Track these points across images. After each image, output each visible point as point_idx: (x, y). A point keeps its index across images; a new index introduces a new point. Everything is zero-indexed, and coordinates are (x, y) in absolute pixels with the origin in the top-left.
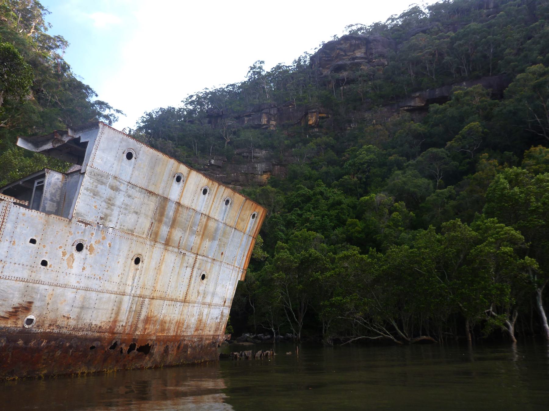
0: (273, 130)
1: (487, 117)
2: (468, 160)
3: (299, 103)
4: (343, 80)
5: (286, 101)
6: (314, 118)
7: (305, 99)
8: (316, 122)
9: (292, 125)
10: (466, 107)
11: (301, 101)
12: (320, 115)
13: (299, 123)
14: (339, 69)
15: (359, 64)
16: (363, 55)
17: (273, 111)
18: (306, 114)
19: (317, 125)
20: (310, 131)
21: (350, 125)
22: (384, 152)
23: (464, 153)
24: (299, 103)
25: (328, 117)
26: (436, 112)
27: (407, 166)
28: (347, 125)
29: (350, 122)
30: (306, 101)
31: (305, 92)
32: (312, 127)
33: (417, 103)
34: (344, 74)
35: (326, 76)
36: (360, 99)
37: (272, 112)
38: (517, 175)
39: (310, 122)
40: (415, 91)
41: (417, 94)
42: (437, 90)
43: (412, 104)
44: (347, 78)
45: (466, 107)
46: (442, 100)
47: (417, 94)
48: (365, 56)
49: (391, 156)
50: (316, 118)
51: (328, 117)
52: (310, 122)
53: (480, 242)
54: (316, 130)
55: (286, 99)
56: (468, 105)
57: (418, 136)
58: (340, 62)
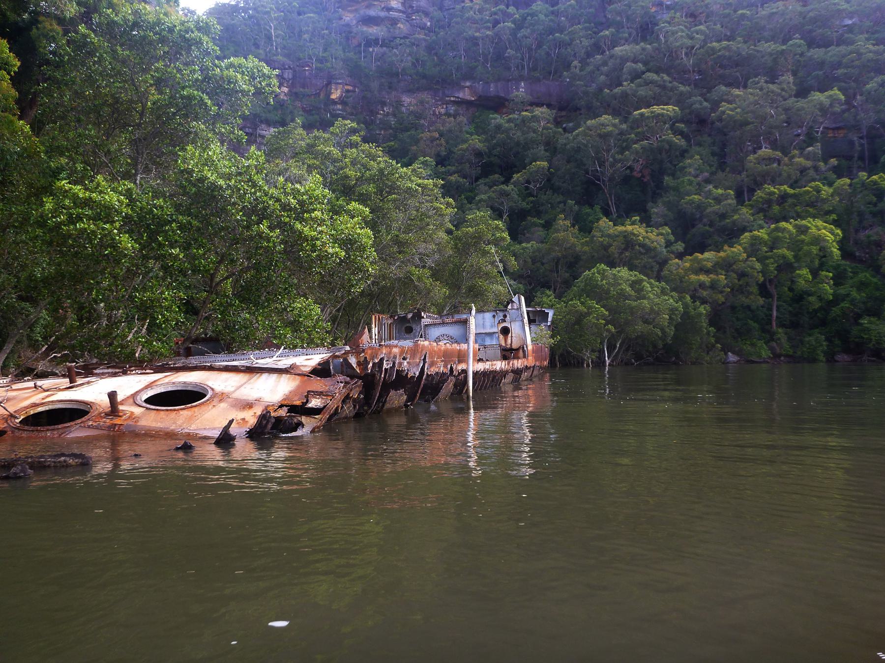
0: (283, 100)
1: (551, 147)
2: (532, 199)
3: (319, 65)
4: (377, 40)
5: (299, 59)
6: (339, 91)
7: (327, 61)
8: (340, 98)
9: (308, 95)
10: (532, 135)
11: (322, 63)
12: (346, 87)
13: (319, 94)
14: (369, 21)
15: (394, 22)
16: (400, 7)
17: (288, 74)
18: (329, 84)
19: (342, 101)
20: (332, 107)
21: (383, 107)
22: (443, 169)
23: (527, 188)
24: (319, 65)
25: (354, 91)
26: (498, 127)
27: (480, 201)
28: (379, 107)
29: (384, 104)
30: (329, 65)
31: (325, 50)
32: (334, 102)
33: (465, 95)
34: (374, 31)
35: (348, 25)
36: (398, 75)
37: (286, 76)
38: (604, 270)
39: (333, 97)
40: (466, 77)
41: (468, 84)
42: (492, 85)
43: (461, 95)
44: (383, 40)
45: (532, 135)
46: (498, 104)
47: (468, 84)
48: (401, 8)
49: (451, 175)
50: (342, 92)
51: (354, 91)
52: (333, 97)
53: (588, 314)
54: (339, 107)
55: (301, 56)
56: (534, 132)
57: (479, 154)
58: (372, 13)
